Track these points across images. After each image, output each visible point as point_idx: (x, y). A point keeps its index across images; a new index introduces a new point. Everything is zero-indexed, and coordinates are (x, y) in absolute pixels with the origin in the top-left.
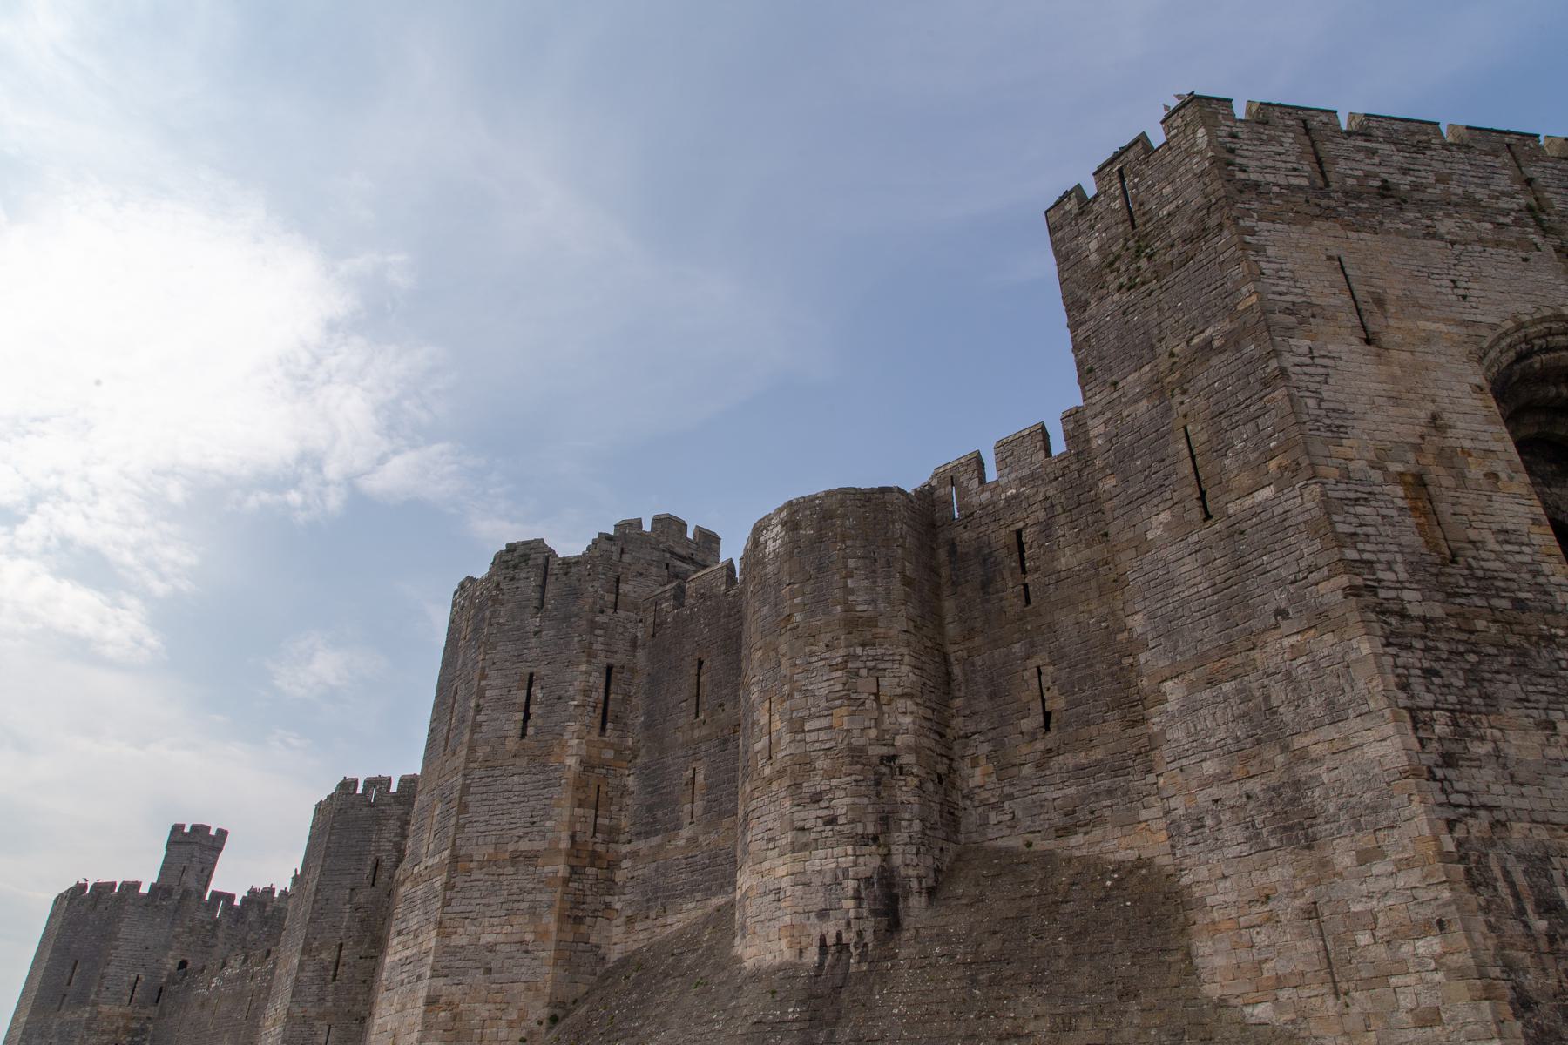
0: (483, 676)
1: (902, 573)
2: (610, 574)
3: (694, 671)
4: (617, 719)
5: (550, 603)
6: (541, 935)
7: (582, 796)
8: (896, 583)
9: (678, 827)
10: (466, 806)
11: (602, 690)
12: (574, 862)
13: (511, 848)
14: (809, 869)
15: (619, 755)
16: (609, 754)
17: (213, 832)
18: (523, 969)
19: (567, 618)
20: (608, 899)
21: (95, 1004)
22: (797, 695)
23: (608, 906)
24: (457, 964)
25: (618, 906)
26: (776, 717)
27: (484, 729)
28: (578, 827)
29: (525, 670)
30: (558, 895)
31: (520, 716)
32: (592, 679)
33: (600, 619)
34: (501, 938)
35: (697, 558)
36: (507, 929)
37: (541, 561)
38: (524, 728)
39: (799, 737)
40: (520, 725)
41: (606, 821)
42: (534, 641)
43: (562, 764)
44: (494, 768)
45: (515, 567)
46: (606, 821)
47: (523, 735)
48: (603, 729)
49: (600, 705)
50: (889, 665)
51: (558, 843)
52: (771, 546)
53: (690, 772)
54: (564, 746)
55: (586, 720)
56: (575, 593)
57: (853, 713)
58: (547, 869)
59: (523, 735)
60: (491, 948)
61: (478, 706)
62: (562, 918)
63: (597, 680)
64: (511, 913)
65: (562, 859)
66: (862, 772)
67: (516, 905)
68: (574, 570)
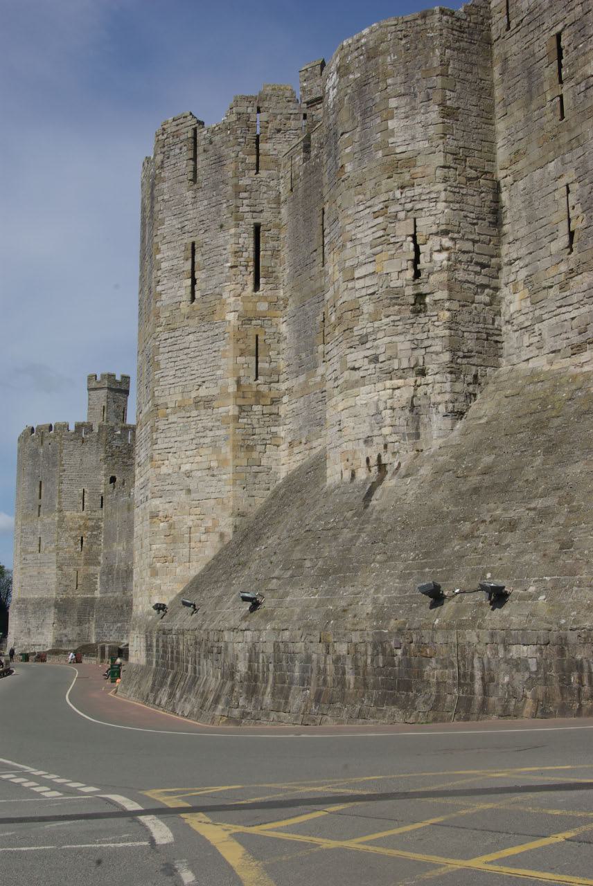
1: (442, 104)
2: (250, 136)
6: (223, 463)
7: (243, 346)
8: (434, 114)
9: (316, 367)
10: (158, 363)
12: (241, 402)
13: (194, 394)
14: (359, 403)
16: (263, 307)
17: (118, 378)
18: (212, 489)
20: (274, 429)
21: (60, 511)
23: (275, 435)
24: (167, 488)
25: (283, 434)
27: (164, 297)
28: (242, 373)
29: (188, 240)
30: (231, 430)
31: (189, 282)
32: (241, 241)
34: (195, 466)
36: (198, 459)
39: (350, 285)
40: (189, 290)
41: (267, 365)
43: (224, 320)
44: (174, 330)
47: (193, 299)
49: (251, 263)
50: (425, 204)
51: (227, 387)
53: (321, 315)
54: (224, 304)
57: (392, 257)
58: (221, 410)
59: (193, 299)
60: (188, 475)
62: (236, 448)
64: (199, 446)
65: (231, 401)
66: (399, 312)
67: (202, 440)
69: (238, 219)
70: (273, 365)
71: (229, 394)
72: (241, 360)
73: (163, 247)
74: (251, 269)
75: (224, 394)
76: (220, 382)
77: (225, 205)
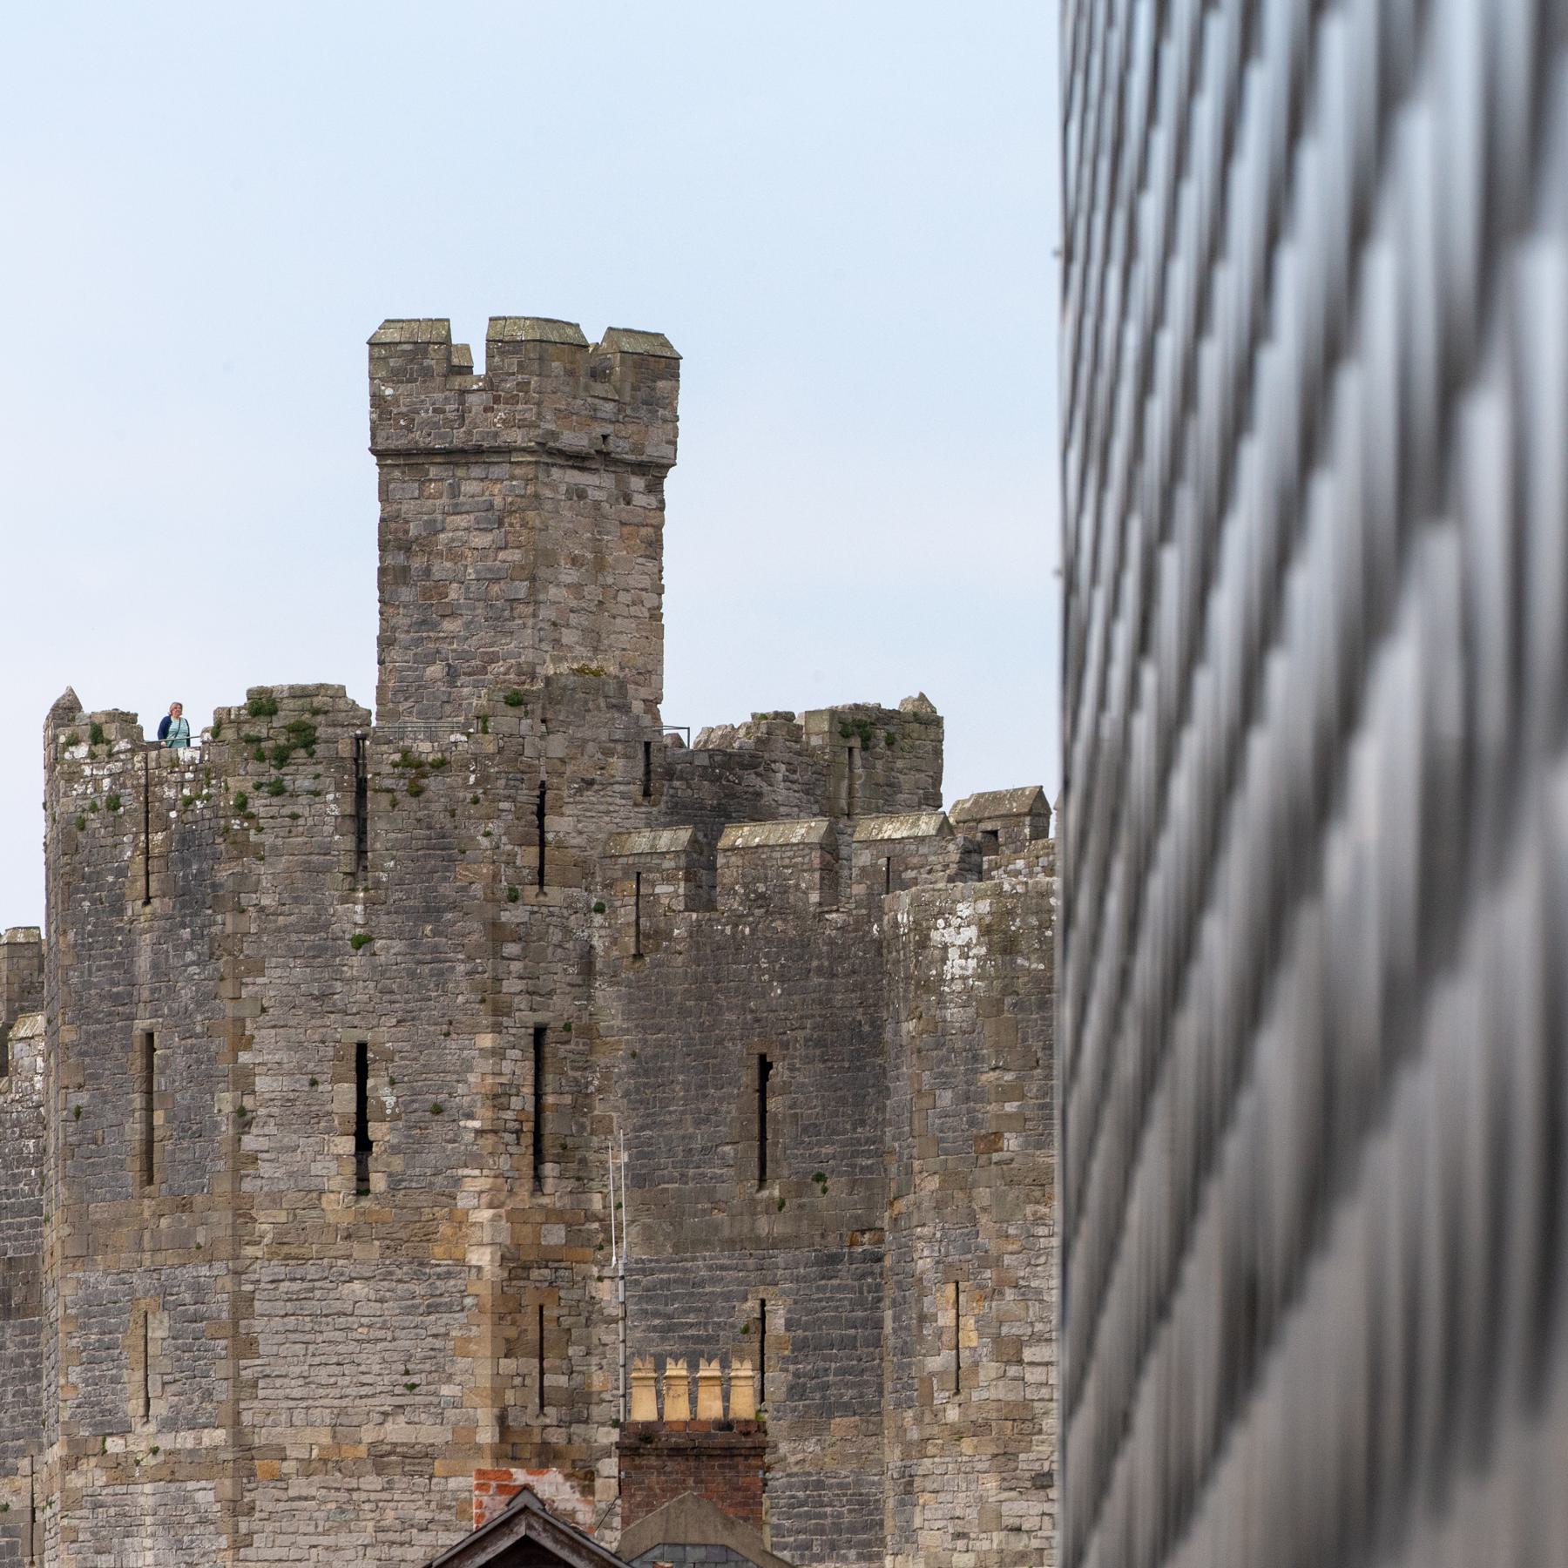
0: (245, 1042)
3: (749, 1077)
4: (565, 1153)
5: (386, 868)
7: (512, 1333)
10: (253, 1343)
11: (528, 1090)
13: (368, 1435)
15: (576, 1236)
16: (555, 1235)
19: (432, 911)
22: (1010, 1294)
26: (969, 1323)
27: (265, 1169)
31: (347, 1145)
32: (507, 1066)
33: (512, 915)
35: (620, 447)
37: (345, 749)
38: (362, 1178)
39: (1013, 1371)
40: (350, 1168)
41: (563, 1380)
42: (356, 963)
43: (461, 1262)
45: (282, 758)
46: (563, 1380)
47: (362, 1189)
48: (538, 1178)
49: (528, 1126)
52: (955, 965)
53: (751, 1305)
54: (460, 1221)
55: (504, 1163)
56: (444, 848)
58: (453, 1483)
59: (362, 1189)
61: (241, 1112)
63: (518, 1066)
67: (397, 1552)
68: (433, 784)
69: (500, 1010)
70: (577, 1379)
71: (479, 1448)
72: (509, 1365)
73: (265, 1036)
74: (528, 1139)
75: (463, 1445)
76: (450, 1413)
77: (461, 968)
